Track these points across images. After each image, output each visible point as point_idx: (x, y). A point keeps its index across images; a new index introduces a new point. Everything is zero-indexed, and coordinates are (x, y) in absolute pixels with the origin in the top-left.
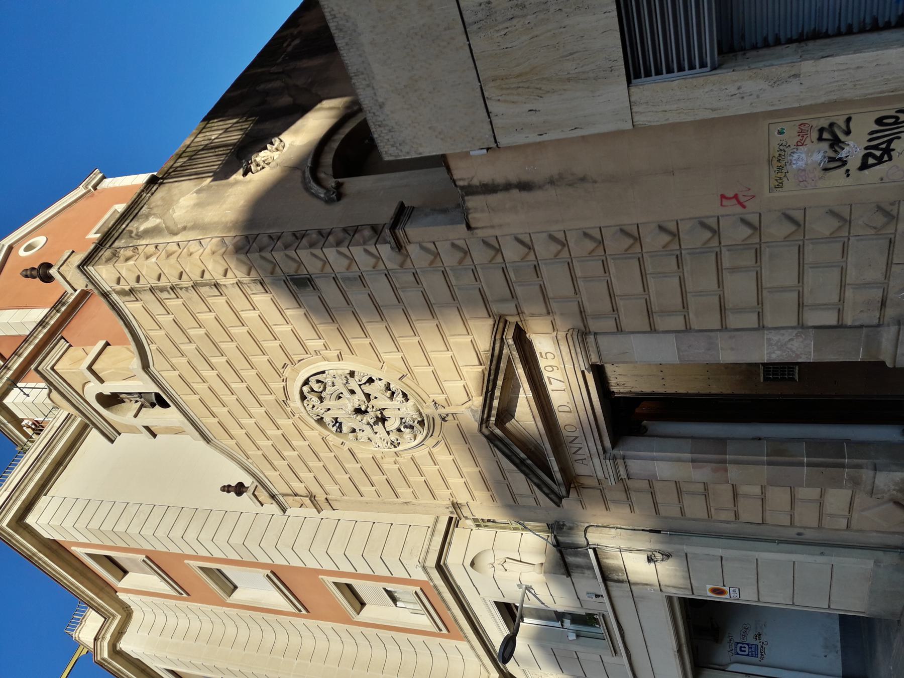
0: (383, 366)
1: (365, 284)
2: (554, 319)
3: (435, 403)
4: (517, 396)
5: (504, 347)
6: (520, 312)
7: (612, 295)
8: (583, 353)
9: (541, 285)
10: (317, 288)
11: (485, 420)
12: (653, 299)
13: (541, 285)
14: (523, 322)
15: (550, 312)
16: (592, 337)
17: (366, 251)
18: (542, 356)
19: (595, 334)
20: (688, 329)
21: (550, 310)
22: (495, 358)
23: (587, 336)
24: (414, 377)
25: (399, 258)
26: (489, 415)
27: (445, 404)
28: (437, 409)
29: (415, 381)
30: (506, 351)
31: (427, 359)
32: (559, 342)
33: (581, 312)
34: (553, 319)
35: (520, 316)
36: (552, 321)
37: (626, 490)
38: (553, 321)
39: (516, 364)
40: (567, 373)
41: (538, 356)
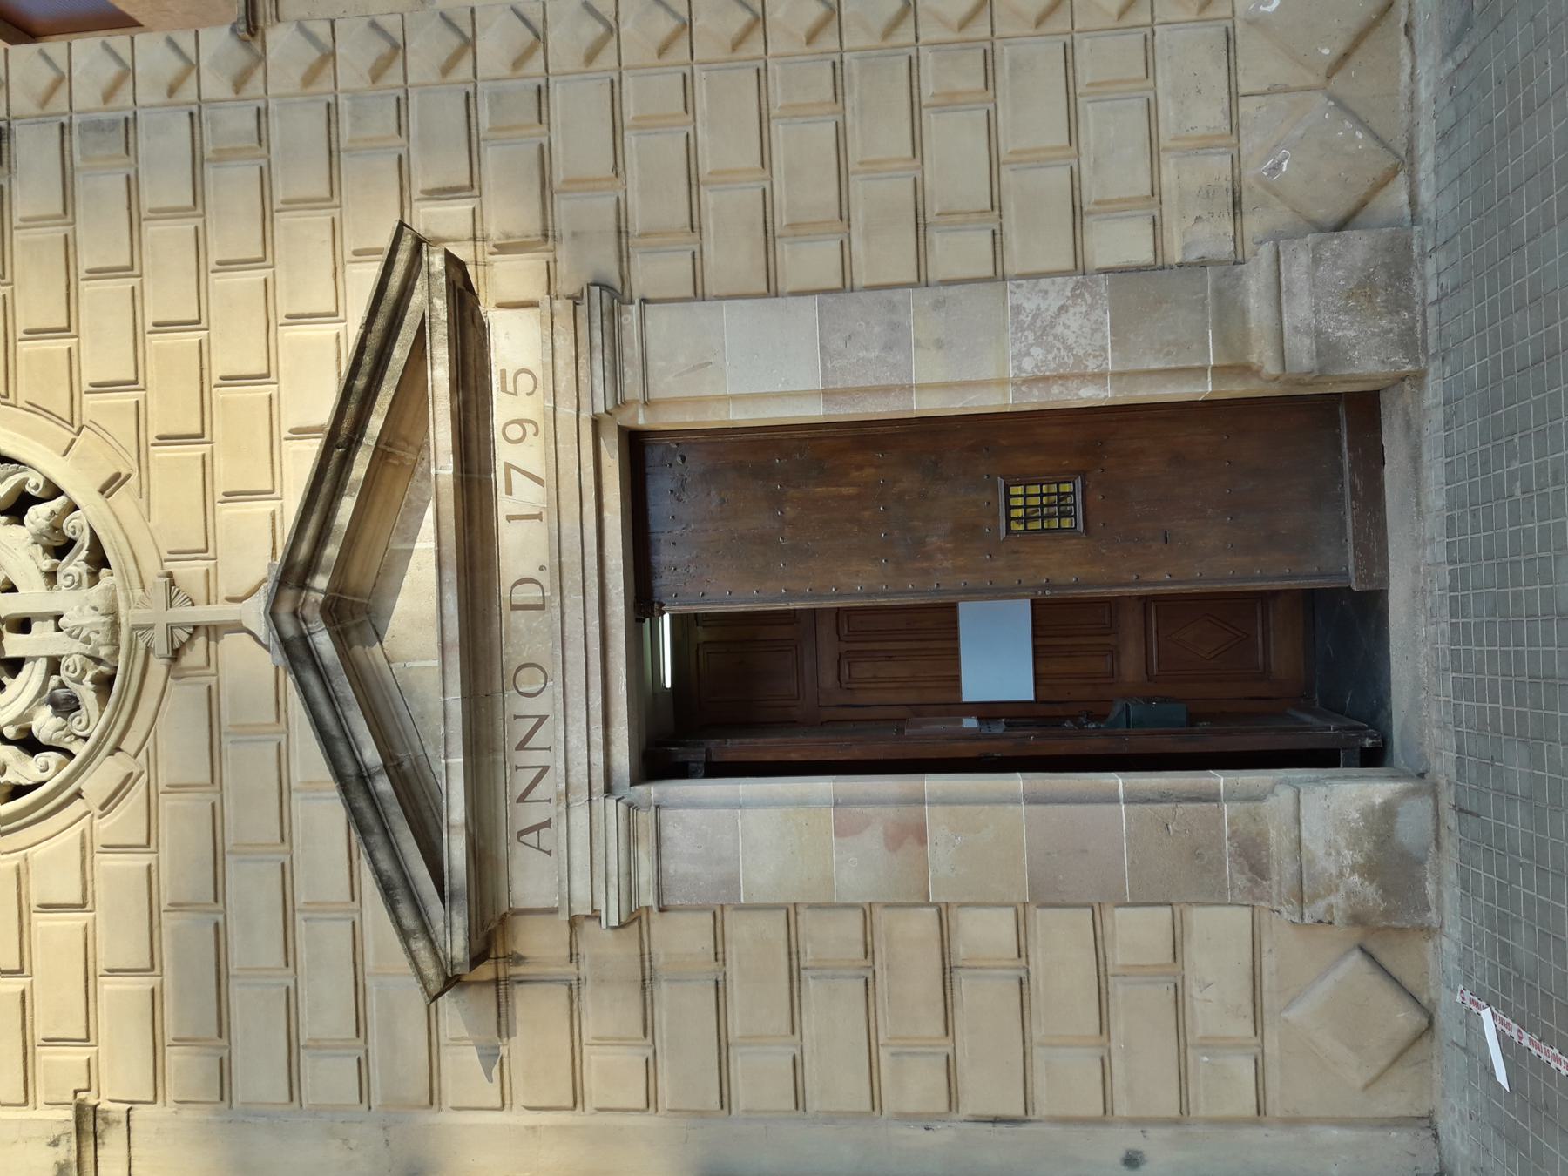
0: (73, 441)
1: (131, 145)
2: (555, 261)
3: (173, 584)
4: (405, 546)
5: (418, 283)
6: (479, 234)
7: (694, 182)
8: (606, 351)
9: (541, 146)
10: (9, 162)
11: (298, 570)
12: (780, 194)
13: (541, 146)
14: (480, 268)
15: (550, 234)
16: (634, 308)
17: (171, 43)
18: (504, 389)
19: (644, 301)
20: (846, 287)
21: (550, 229)
22: (386, 308)
23: (623, 306)
24: (144, 493)
25: (241, 57)
26: (311, 567)
27: (198, 591)
28: (170, 603)
29: (143, 502)
30: (417, 299)
31: (202, 384)
32: (555, 319)
33: (619, 232)
34: (551, 260)
35: (475, 246)
36: (548, 263)
37: (644, 980)
38: (552, 265)
39: (435, 343)
40: (558, 437)
41: (496, 385)
